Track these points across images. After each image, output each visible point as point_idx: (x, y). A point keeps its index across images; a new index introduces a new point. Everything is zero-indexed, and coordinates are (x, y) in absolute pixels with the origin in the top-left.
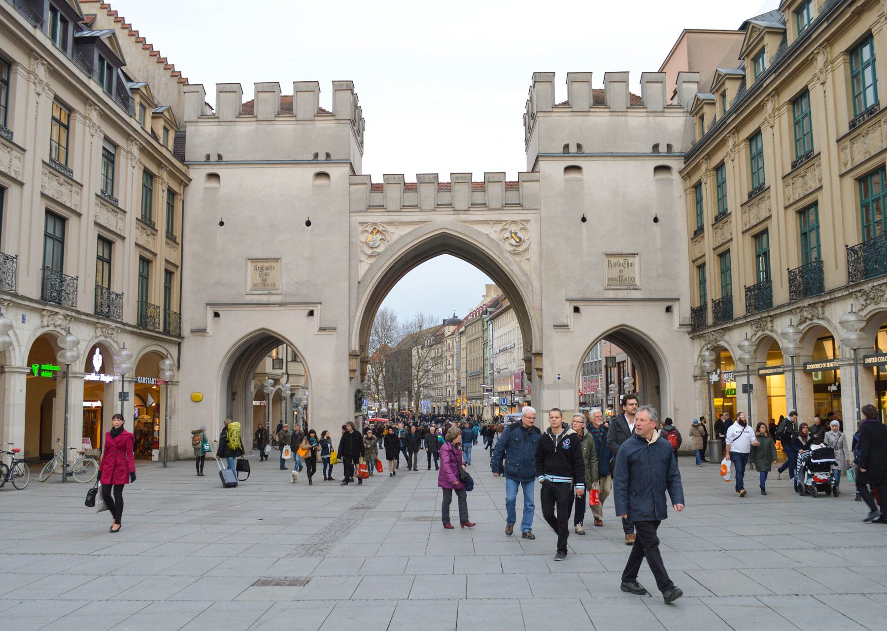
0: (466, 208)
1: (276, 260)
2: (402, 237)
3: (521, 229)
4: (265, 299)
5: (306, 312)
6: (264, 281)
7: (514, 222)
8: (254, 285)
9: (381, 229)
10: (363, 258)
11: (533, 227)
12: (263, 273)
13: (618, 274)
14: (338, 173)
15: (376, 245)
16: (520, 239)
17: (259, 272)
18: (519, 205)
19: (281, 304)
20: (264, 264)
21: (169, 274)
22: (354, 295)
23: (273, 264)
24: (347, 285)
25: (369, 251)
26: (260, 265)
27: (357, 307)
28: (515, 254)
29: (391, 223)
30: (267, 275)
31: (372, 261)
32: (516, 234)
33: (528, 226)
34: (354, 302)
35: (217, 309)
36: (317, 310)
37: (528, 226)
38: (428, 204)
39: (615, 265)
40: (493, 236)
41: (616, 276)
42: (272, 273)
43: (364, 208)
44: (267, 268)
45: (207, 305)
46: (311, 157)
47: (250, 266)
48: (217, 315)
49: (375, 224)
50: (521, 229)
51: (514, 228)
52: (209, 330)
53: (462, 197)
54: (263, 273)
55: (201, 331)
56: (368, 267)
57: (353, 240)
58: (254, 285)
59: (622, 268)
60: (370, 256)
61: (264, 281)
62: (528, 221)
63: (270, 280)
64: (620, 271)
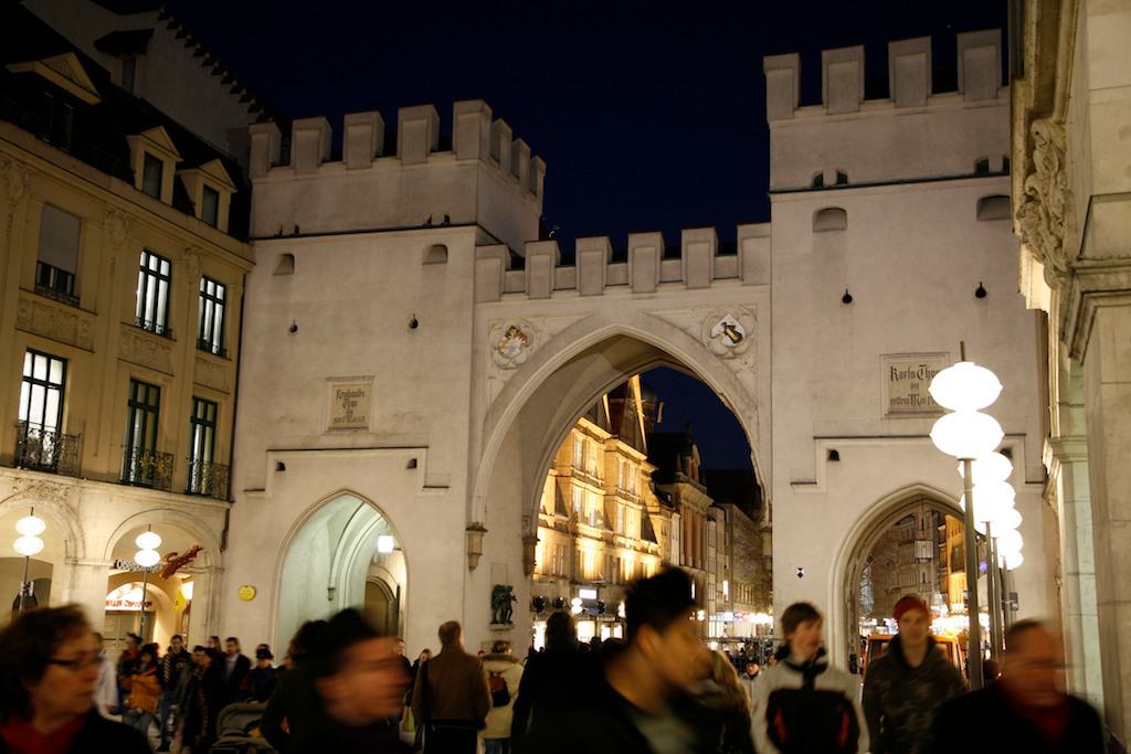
8: (336, 420)
10: (495, 372)
12: (349, 399)
13: (910, 392)
15: (514, 353)
16: (739, 335)
17: (341, 401)
30: (354, 404)
32: (732, 328)
39: (903, 375)
40: (695, 330)
41: (905, 396)
42: (361, 401)
44: (355, 394)
48: (281, 467)
54: (349, 399)
56: (501, 386)
59: (916, 380)
63: (357, 412)
64: (913, 386)
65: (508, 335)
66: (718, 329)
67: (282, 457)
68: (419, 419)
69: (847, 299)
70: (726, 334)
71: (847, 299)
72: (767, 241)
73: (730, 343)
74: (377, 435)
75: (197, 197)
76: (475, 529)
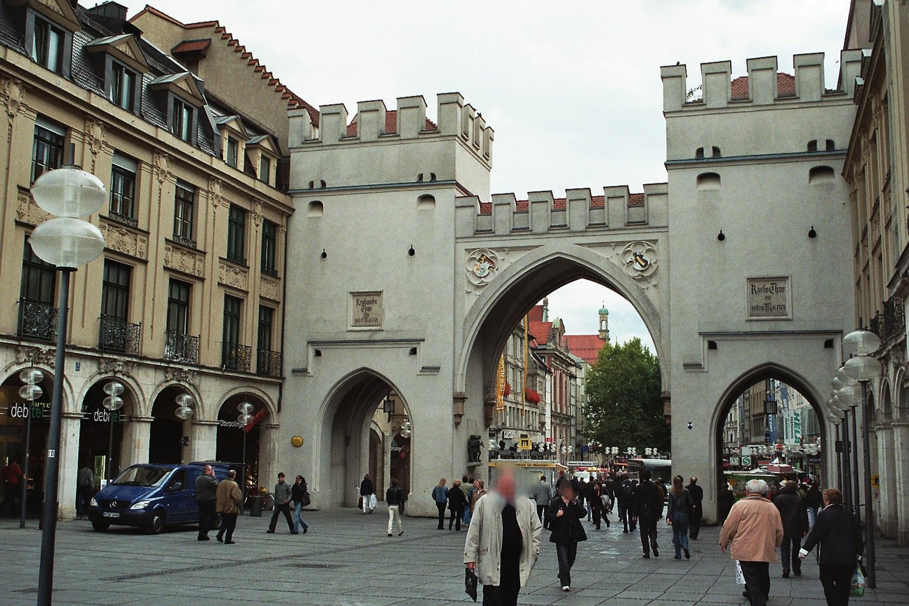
0: (582, 228)
1: (379, 293)
2: (513, 265)
3: (648, 251)
4: (365, 336)
5: (409, 349)
6: (366, 316)
7: (639, 243)
8: (357, 321)
9: (489, 255)
11: (660, 247)
14: (445, 197)
16: (646, 262)
17: (360, 307)
18: (643, 223)
19: (383, 341)
20: (367, 300)
21: (267, 312)
22: (460, 330)
23: (376, 298)
24: (451, 319)
25: (476, 282)
26: (362, 299)
27: (464, 341)
28: (639, 280)
29: (500, 249)
30: (370, 309)
31: (479, 292)
32: (641, 257)
33: (655, 247)
34: (459, 339)
35: (317, 348)
36: (421, 348)
37: (655, 247)
38: (541, 227)
40: (615, 261)
42: (375, 308)
43: (471, 233)
44: (369, 303)
45: (309, 343)
46: (414, 179)
47: (352, 301)
49: (482, 251)
50: (648, 251)
51: (639, 250)
52: (310, 370)
53: (577, 216)
55: (301, 372)
57: (459, 269)
58: (357, 321)
60: (478, 287)
61: (366, 316)
62: (655, 241)
63: (372, 315)
65: (480, 259)
66: (631, 257)
67: (317, 348)
68: (417, 319)
69: (721, 237)
70: (637, 260)
71: (721, 237)
72: (664, 197)
73: (637, 266)
74: (388, 332)
75: (258, 164)
76: (459, 399)
